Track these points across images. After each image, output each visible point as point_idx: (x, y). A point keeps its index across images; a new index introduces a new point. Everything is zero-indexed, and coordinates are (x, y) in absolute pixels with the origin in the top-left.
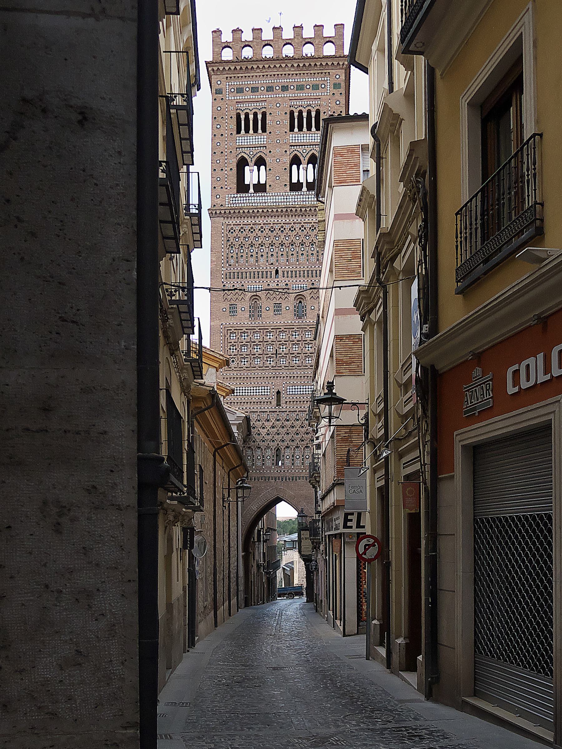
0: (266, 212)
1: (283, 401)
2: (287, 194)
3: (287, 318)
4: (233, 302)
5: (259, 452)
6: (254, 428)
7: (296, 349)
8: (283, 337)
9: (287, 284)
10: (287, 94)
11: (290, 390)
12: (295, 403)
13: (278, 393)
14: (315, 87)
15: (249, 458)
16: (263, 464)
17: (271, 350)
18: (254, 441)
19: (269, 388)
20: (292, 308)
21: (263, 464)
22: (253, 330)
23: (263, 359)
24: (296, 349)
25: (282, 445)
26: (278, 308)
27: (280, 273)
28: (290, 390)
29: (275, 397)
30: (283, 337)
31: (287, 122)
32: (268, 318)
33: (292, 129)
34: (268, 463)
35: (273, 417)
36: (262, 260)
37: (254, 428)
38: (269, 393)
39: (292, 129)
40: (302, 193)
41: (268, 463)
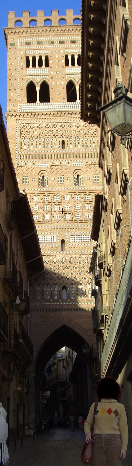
2: (64, 103)
3: (69, 185)
10: (63, 45)
13: (63, 241)
19: (55, 237)
26: (60, 180)
29: (60, 244)
31: (64, 61)
33: (67, 64)
38: (55, 241)
39: (67, 64)
40: (76, 103)
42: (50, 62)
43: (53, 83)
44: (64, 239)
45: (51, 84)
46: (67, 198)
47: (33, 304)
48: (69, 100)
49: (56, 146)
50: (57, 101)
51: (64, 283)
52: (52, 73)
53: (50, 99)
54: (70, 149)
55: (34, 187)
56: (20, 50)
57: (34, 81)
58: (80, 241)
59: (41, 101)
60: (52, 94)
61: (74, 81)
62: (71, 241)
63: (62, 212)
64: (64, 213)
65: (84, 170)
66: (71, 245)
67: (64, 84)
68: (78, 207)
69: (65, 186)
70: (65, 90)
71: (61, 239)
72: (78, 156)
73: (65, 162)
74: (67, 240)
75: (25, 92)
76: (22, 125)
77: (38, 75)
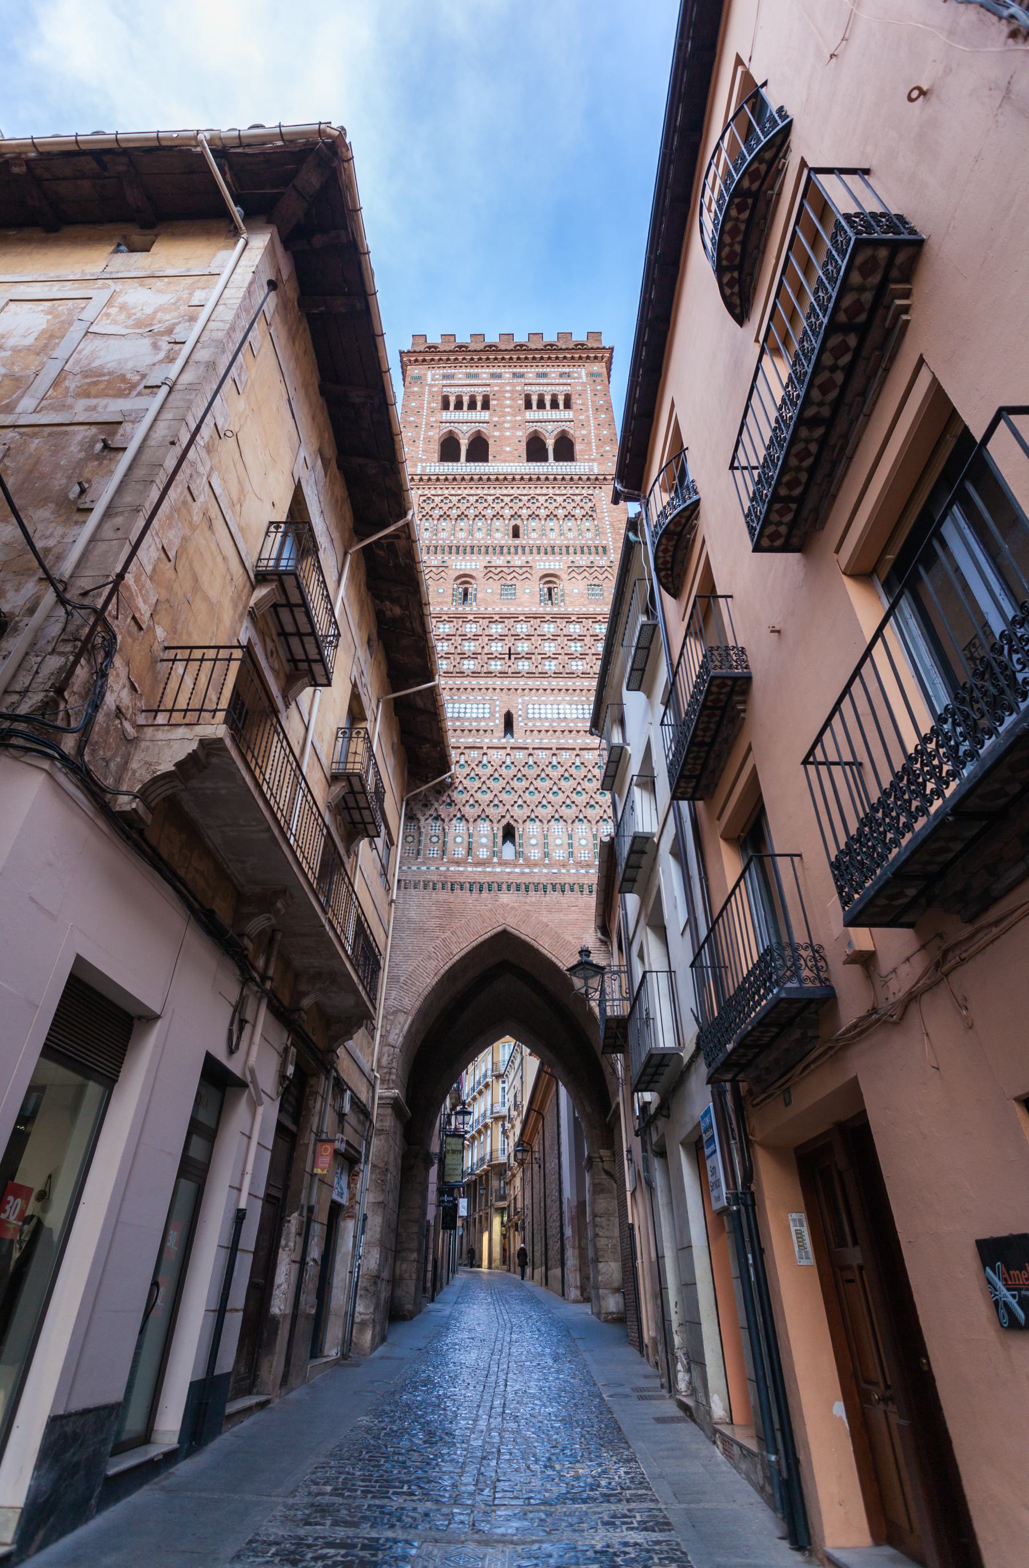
1: (518, 724)
14: (561, 375)
19: (487, 706)
25: (519, 813)
31: (521, 402)
35: (497, 756)
41: (483, 854)
42: (493, 403)
43: (497, 434)
44: (513, 711)
46: (522, 629)
47: (414, 868)
48: (529, 460)
49: (498, 535)
50: (505, 461)
51: (508, 816)
52: (495, 419)
53: (490, 458)
54: (531, 536)
55: (441, 603)
56: (431, 386)
57: (456, 431)
58: (556, 716)
59: (468, 460)
61: (544, 432)
62: (530, 716)
63: (510, 654)
64: (513, 657)
65: (564, 576)
66: (530, 724)
67: (522, 435)
68: (549, 648)
69: (518, 605)
70: (524, 444)
71: (504, 711)
72: (551, 550)
73: (518, 560)
74: (520, 713)
75: (436, 447)
76: (422, 498)
77: (464, 424)
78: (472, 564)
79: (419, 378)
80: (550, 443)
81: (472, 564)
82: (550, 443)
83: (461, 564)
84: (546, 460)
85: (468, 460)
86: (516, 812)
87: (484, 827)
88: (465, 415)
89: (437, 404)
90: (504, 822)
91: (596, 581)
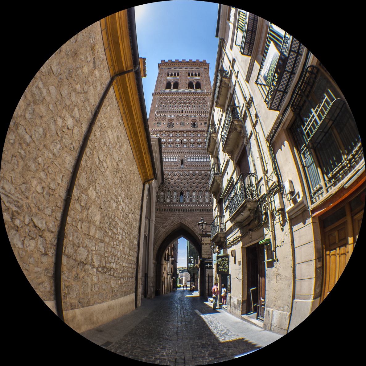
0: (178, 94)
1: (185, 163)
4: (159, 121)
5: (168, 194)
6: (166, 179)
7: (192, 140)
8: (185, 135)
9: (187, 115)
11: (189, 159)
12: (192, 166)
15: (162, 197)
16: (171, 201)
17: (178, 140)
18: (166, 187)
19: (176, 158)
20: (190, 124)
21: (171, 201)
22: (169, 132)
23: (174, 144)
24: (192, 140)
27: (184, 112)
28: (189, 159)
30: (185, 135)
32: (177, 127)
34: (175, 200)
36: (175, 108)
37: (166, 179)
38: (176, 161)
41: (175, 200)
45: (180, 82)
59: (173, 88)
60: (179, 86)
78: (173, 116)
79: (163, 69)
80: (194, 84)
81: (173, 116)
82: (194, 84)
83: (169, 116)
84: (193, 88)
85: (173, 88)
86: (183, 189)
87: (175, 194)
88: (173, 77)
89: (166, 75)
90: (180, 191)
91: (206, 122)
